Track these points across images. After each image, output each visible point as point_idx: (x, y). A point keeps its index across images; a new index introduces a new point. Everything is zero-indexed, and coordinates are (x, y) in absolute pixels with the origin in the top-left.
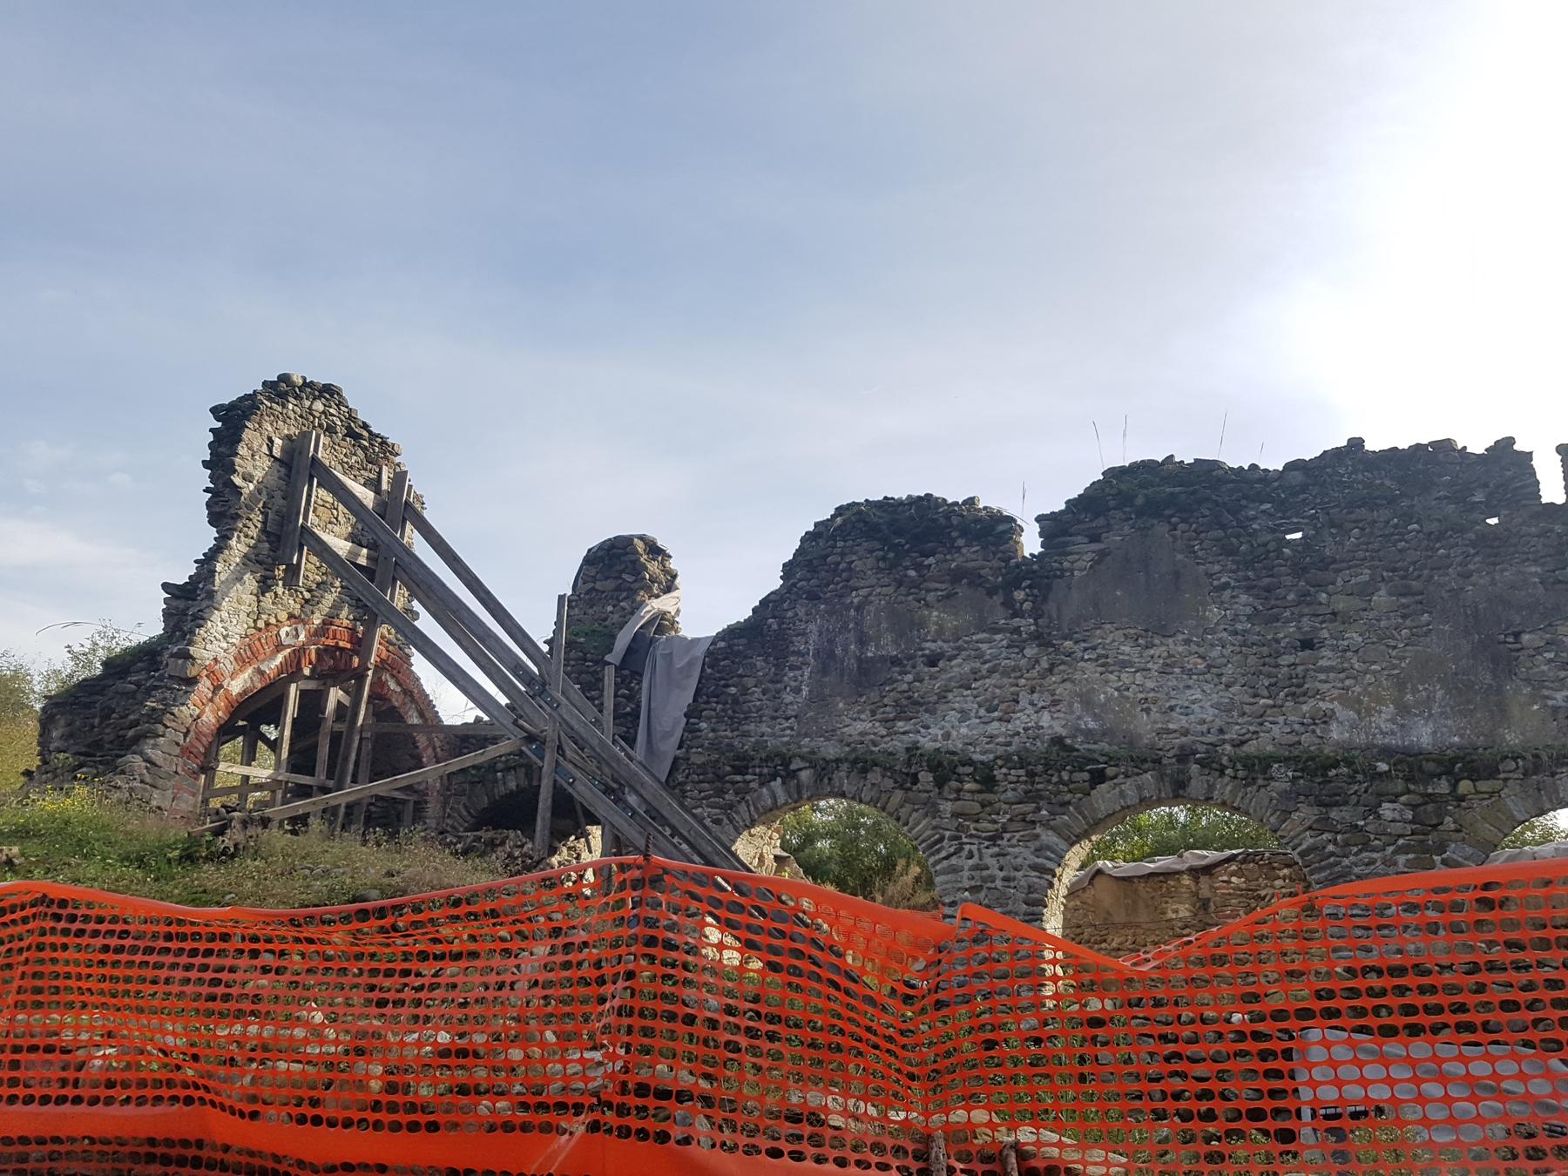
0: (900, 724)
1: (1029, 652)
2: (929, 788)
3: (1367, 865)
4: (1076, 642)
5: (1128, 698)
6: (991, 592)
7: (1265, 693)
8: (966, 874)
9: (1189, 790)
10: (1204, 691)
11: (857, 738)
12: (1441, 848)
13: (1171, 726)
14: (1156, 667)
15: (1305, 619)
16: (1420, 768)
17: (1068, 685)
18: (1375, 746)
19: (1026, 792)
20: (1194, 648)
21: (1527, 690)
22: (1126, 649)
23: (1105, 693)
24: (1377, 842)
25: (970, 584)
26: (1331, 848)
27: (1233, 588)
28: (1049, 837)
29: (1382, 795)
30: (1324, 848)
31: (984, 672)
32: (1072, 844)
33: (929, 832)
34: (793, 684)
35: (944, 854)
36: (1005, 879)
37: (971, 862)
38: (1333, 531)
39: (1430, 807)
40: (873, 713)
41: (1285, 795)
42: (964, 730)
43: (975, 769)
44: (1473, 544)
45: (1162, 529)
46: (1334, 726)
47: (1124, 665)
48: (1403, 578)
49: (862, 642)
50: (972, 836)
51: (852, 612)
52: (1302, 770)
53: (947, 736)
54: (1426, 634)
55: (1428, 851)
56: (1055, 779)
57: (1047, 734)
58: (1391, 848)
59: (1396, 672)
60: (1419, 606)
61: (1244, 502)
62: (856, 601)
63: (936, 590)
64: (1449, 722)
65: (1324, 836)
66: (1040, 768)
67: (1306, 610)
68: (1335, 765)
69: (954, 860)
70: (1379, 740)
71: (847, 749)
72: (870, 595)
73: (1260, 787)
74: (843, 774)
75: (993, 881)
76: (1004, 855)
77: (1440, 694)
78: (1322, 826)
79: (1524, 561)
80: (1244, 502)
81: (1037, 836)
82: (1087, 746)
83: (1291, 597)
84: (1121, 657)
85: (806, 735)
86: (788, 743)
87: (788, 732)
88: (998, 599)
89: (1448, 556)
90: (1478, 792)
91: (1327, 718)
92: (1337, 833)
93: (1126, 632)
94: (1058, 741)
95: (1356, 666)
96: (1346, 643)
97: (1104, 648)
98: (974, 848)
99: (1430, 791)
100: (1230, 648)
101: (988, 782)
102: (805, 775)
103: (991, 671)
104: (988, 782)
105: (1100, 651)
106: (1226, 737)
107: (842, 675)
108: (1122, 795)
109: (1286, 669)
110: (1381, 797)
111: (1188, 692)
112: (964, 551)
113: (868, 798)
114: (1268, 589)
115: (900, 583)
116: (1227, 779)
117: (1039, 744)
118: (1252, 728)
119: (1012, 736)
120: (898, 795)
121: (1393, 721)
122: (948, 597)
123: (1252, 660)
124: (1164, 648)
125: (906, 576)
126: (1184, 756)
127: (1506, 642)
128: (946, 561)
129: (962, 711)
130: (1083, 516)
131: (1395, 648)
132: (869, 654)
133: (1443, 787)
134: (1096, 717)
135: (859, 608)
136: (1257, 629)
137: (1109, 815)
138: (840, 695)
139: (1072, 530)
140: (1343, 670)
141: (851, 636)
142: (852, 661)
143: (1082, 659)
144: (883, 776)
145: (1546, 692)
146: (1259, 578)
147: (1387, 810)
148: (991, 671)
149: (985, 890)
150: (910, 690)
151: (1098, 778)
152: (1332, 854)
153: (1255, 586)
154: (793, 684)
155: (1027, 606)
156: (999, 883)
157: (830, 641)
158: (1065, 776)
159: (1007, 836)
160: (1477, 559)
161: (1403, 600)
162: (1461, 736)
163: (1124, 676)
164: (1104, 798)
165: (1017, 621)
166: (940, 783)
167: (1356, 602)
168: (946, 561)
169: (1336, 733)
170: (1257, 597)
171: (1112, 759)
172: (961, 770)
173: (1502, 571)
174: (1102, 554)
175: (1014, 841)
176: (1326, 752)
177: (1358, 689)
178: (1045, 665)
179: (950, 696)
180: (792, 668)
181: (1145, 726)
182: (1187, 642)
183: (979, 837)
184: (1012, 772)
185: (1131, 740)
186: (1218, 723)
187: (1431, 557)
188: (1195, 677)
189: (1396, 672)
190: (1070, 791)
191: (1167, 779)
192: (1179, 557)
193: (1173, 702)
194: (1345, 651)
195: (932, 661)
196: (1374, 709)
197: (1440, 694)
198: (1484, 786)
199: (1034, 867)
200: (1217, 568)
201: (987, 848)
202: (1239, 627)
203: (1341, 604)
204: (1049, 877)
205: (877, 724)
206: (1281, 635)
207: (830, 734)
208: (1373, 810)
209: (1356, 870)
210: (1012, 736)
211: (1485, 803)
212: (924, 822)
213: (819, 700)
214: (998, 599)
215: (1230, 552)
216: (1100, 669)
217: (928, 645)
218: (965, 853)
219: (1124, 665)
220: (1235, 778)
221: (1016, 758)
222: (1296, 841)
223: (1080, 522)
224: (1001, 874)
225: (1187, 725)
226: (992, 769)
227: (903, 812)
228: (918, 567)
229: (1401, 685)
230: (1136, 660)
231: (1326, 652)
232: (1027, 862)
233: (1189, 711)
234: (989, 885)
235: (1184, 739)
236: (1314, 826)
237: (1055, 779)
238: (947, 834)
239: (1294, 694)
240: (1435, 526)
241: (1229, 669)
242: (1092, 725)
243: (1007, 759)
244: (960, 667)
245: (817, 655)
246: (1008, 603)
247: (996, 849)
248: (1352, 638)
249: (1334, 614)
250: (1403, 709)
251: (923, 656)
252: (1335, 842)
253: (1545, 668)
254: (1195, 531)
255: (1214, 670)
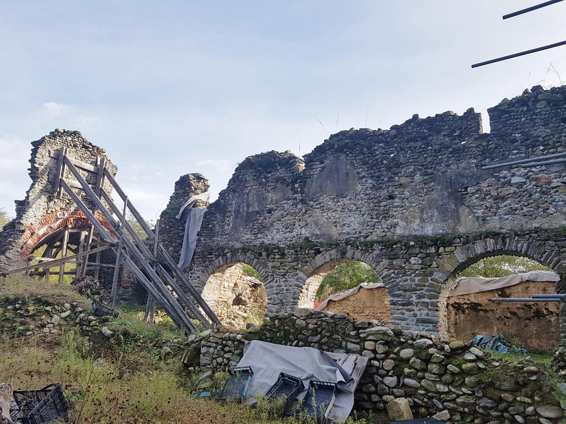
0: (259, 235)
1: (299, 206)
2: (265, 258)
3: (405, 281)
4: (314, 202)
5: (329, 222)
6: (287, 186)
7: (375, 217)
8: (275, 288)
9: (346, 255)
10: (355, 217)
11: (246, 241)
12: (431, 274)
13: (344, 231)
14: (339, 209)
15: (390, 187)
16: (425, 244)
17: (311, 218)
18: (412, 235)
19: (295, 258)
20: (352, 201)
21: (468, 210)
22: (330, 203)
23: (322, 220)
24: (409, 273)
25: (281, 183)
26: (393, 275)
27: (366, 177)
28: (301, 274)
29: (411, 255)
30: (390, 275)
31: (285, 215)
32: (308, 277)
33: (264, 274)
34: (228, 222)
35: (268, 281)
36: (287, 290)
37: (276, 284)
38: (403, 152)
39: (428, 258)
40: (251, 231)
41: (378, 255)
42: (278, 236)
43: (279, 250)
44: (451, 153)
45: (343, 157)
46: (398, 228)
47: (329, 209)
48: (426, 168)
49: (248, 206)
50: (277, 275)
51: (246, 196)
52: (385, 246)
53: (273, 238)
54: (433, 190)
55: (427, 276)
56: (303, 253)
57: (303, 236)
58: (413, 275)
59: (421, 206)
60: (431, 179)
61: (373, 144)
62: (247, 191)
63: (271, 186)
64: (439, 225)
65: (391, 271)
66: (299, 249)
67: (390, 184)
68: (396, 243)
69: (271, 284)
70: (413, 233)
71: (243, 245)
72: (251, 189)
73: (370, 253)
74: (240, 254)
75: (283, 291)
76: (287, 281)
77: (436, 214)
78: (391, 267)
79: (470, 158)
80: (373, 144)
81: (297, 274)
82: (316, 240)
83: (386, 179)
84: (328, 206)
85: (231, 241)
86: (226, 244)
87: (226, 240)
88: (290, 188)
89: (442, 158)
90: (446, 252)
91: (395, 226)
92: (395, 269)
93: (330, 197)
94: (307, 239)
95: (407, 205)
96: (404, 196)
97: (323, 203)
98: (278, 279)
99: (428, 252)
100: (364, 200)
101: (283, 255)
102: (229, 255)
103: (287, 214)
104: (283, 255)
105: (322, 205)
106: (362, 234)
107: (242, 218)
108: (325, 258)
109: (383, 207)
110: (411, 255)
111: (350, 218)
112: (280, 170)
113: (246, 262)
114: (378, 177)
115: (260, 184)
116: (359, 250)
117: (301, 240)
118: (370, 231)
119: (293, 238)
120: (256, 260)
121: (419, 225)
122: (274, 188)
123: (371, 205)
124: (342, 202)
125: (262, 181)
126: (347, 243)
127: (461, 191)
128: (274, 175)
129: (277, 229)
130: (318, 154)
131: (421, 196)
132: (250, 211)
133: (433, 250)
134: (319, 229)
135: (248, 194)
136: (374, 192)
137: (320, 266)
138: (241, 225)
139: (314, 160)
140: (403, 207)
141: (245, 204)
142: (245, 213)
143: (316, 208)
144: (251, 254)
145: (475, 211)
146: (375, 173)
147: (413, 260)
148: (287, 214)
149: (280, 294)
150: (262, 223)
151: (318, 252)
152: (393, 277)
153: (374, 176)
154: (228, 222)
155: (299, 189)
156: (285, 291)
157: (239, 207)
158: (307, 251)
159: (288, 274)
160: (453, 158)
161: (425, 178)
162: (443, 230)
163: (329, 213)
164: (319, 260)
165: (296, 195)
166: (268, 256)
167: (409, 180)
168: (274, 175)
169: (399, 231)
170: (374, 180)
171: (322, 245)
172: (274, 251)
173: (462, 163)
174: (323, 168)
175: (290, 276)
176: (395, 239)
177: (407, 213)
178: (304, 211)
179: (274, 224)
180: (227, 217)
181: (334, 232)
182: (350, 199)
183: (279, 275)
184: (290, 251)
185: (330, 237)
186: (359, 229)
187: (436, 159)
188: (352, 212)
189: (421, 206)
190: (308, 257)
191: (339, 251)
192: (349, 167)
193: (345, 222)
194: (403, 199)
195: (270, 212)
196: (412, 221)
197: (436, 214)
198: (448, 249)
199: (296, 285)
200: (361, 170)
201: (282, 279)
202: (368, 192)
203: (403, 180)
204: (301, 289)
205: (252, 235)
206: (382, 194)
207: (237, 240)
208: (408, 261)
209: (401, 284)
210: (293, 238)
211: (449, 256)
212: (263, 270)
213: (235, 228)
214: (290, 188)
215: (365, 163)
216: (321, 211)
217: (268, 206)
218: (275, 281)
219: (329, 209)
220: (362, 250)
221: (291, 246)
222: (381, 273)
223: (316, 156)
224: (286, 288)
225: (349, 231)
226: (284, 250)
227: (257, 267)
228: (266, 178)
229: (422, 211)
230: (333, 207)
231: (397, 200)
232: (294, 284)
233: (350, 225)
234: (282, 292)
235: (347, 236)
236: (388, 267)
237: (303, 253)
238: (270, 274)
239: (385, 217)
240: (437, 147)
241: (363, 209)
242: (318, 232)
243: (289, 246)
244: (277, 214)
245: (235, 212)
246: (293, 189)
247: (284, 279)
248: (406, 194)
249: (401, 185)
250: (423, 220)
251: (266, 210)
252: (394, 273)
253: (475, 201)
254: (354, 156)
255: (359, 209)
